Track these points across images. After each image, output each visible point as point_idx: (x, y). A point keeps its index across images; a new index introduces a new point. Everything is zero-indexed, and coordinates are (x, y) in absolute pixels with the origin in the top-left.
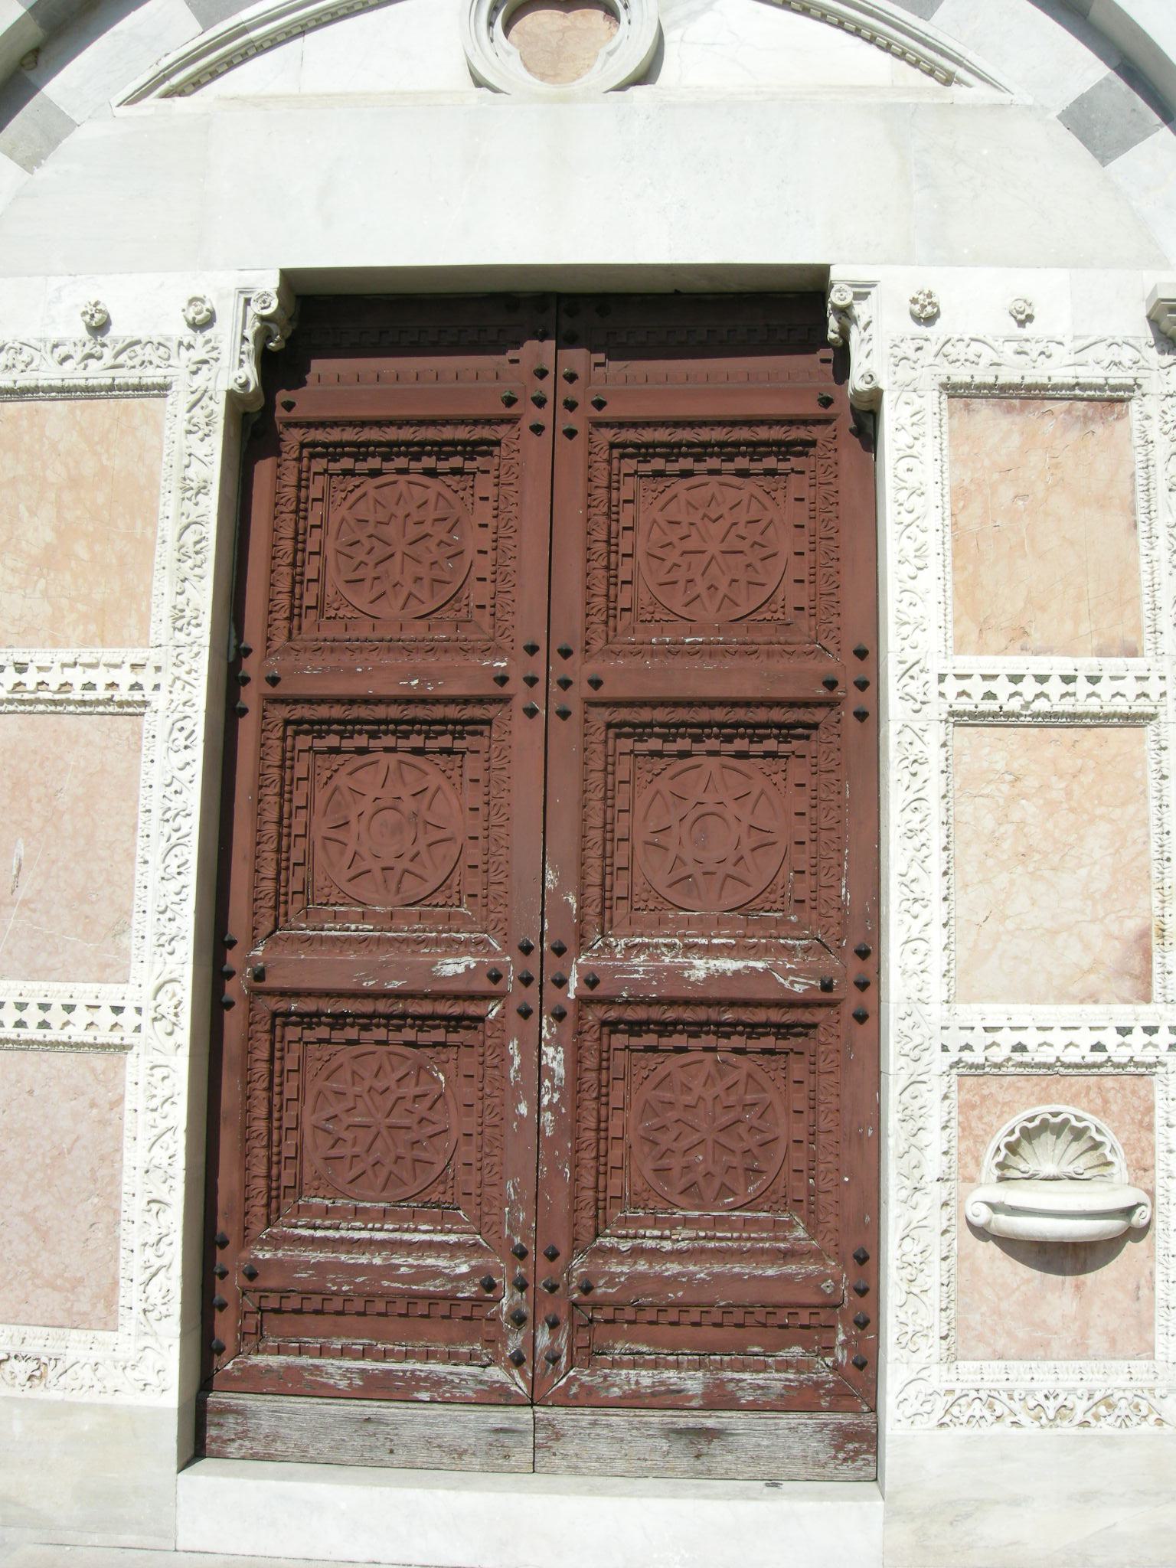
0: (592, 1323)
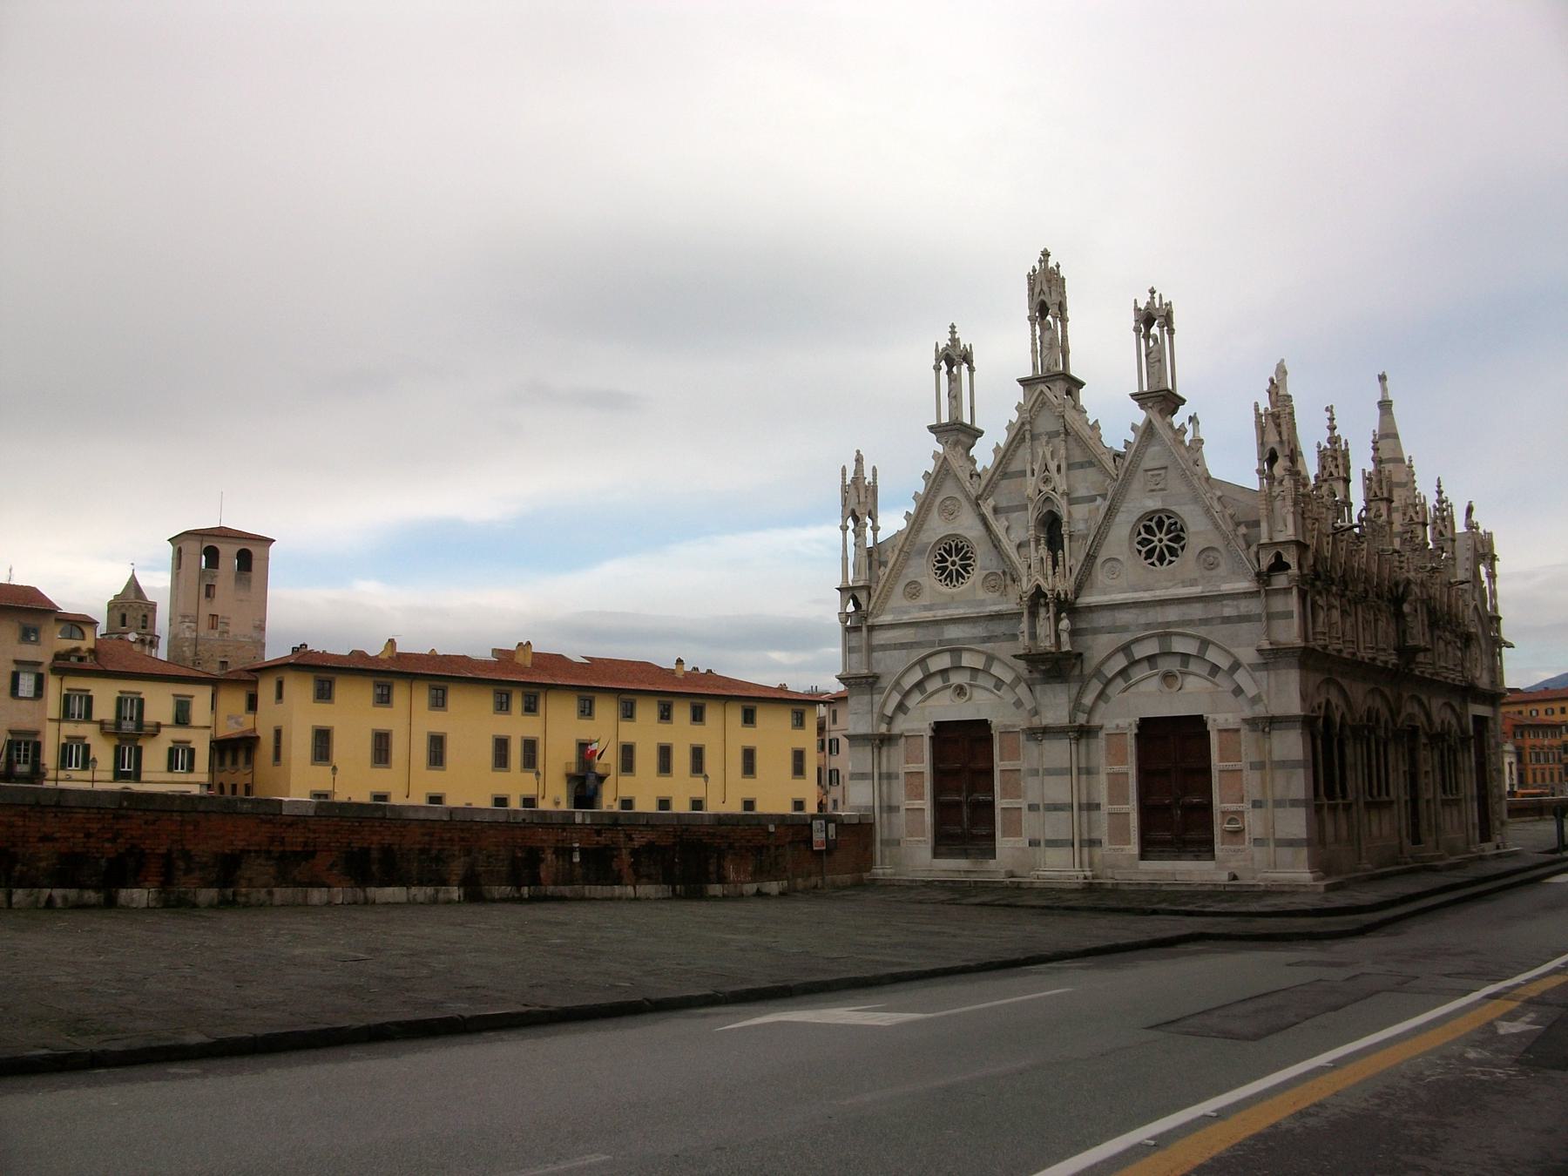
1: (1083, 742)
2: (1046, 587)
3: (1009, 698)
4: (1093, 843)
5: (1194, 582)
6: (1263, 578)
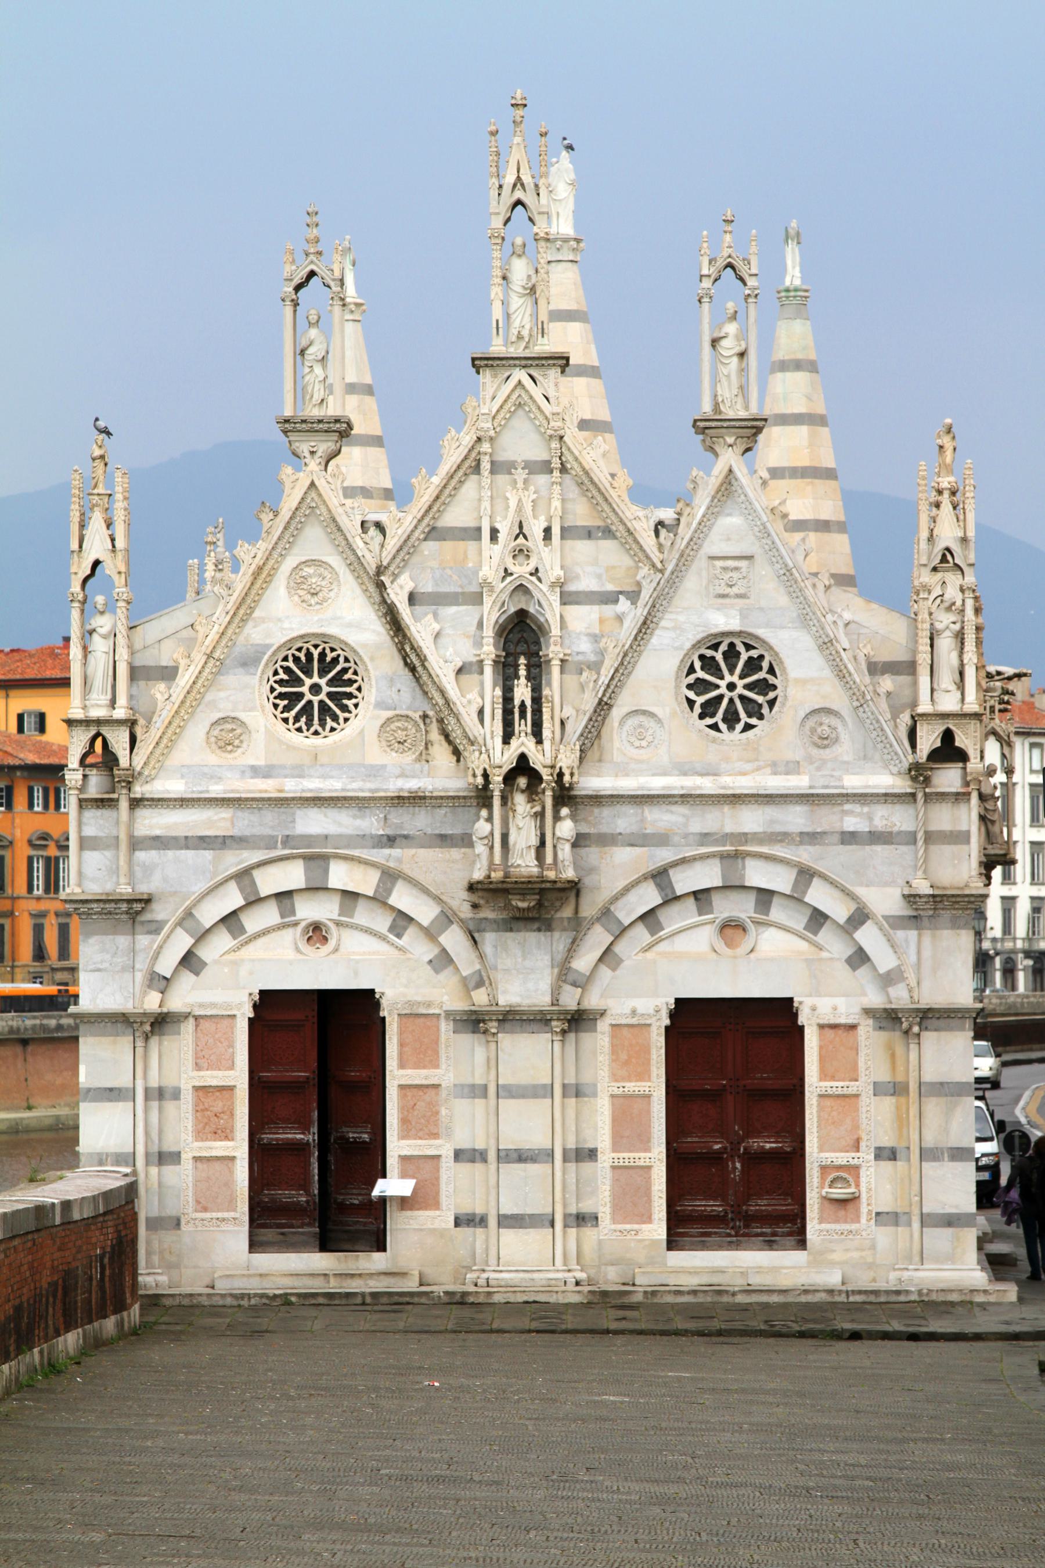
0: (749, 1220)
1: (572, 1036)
2: (538, 760)
3: (423, 951)
4: (582, 1219)
5: (792, 768)
6: (919, 773)
